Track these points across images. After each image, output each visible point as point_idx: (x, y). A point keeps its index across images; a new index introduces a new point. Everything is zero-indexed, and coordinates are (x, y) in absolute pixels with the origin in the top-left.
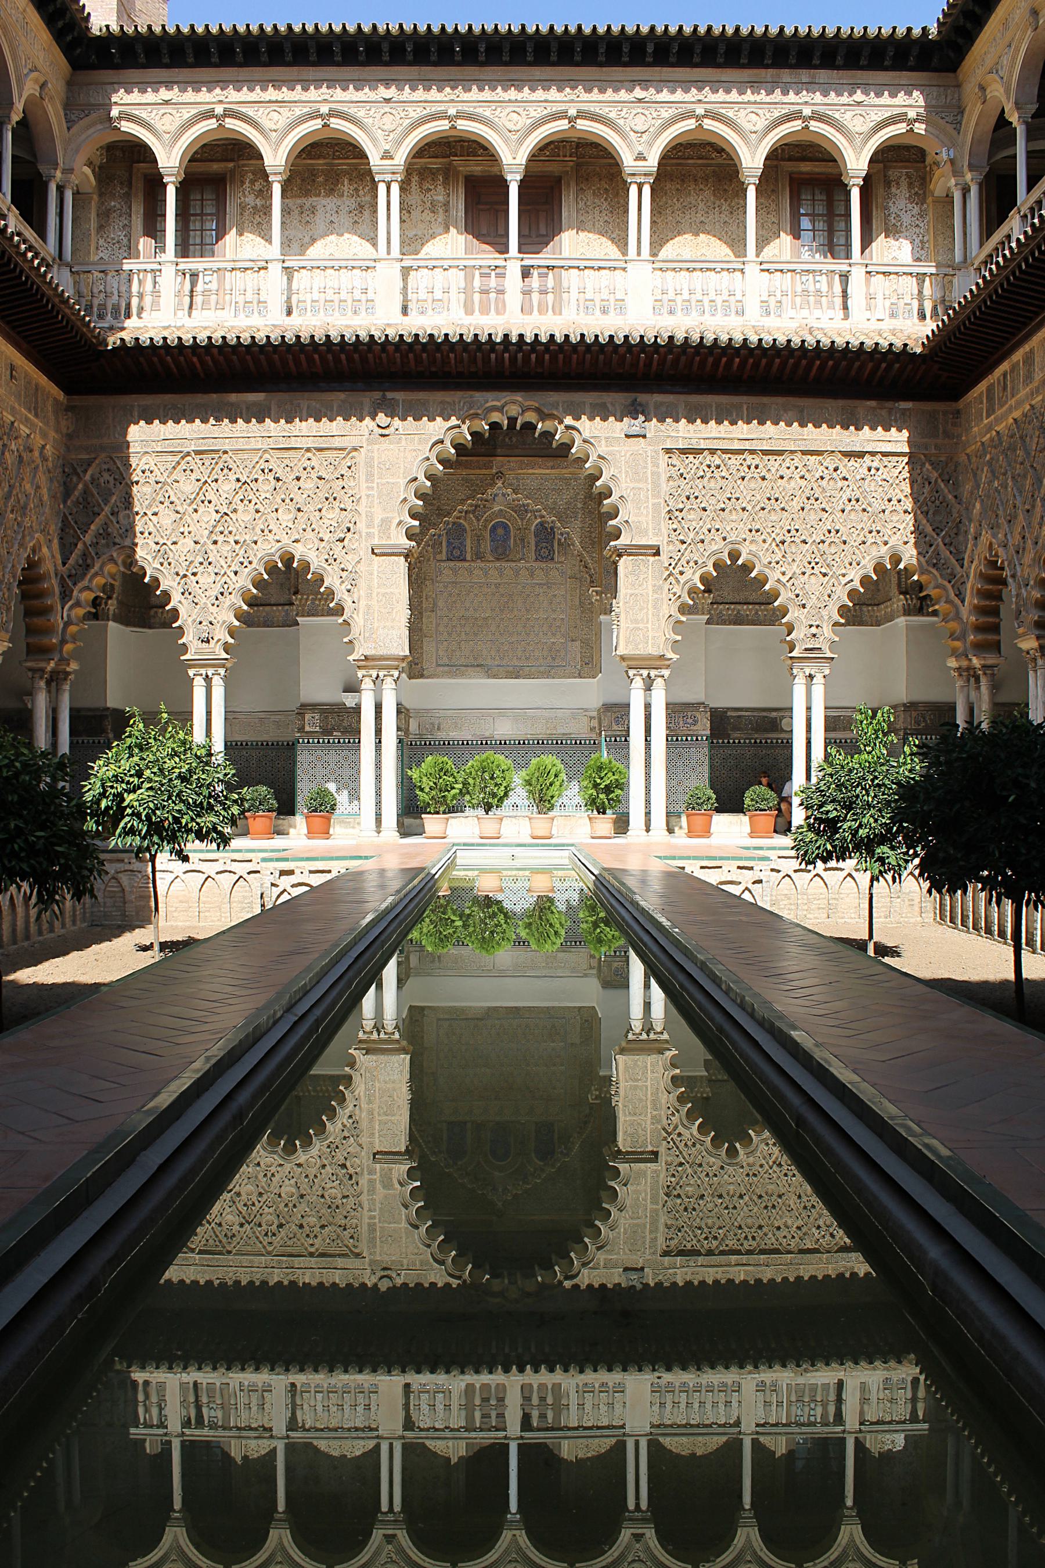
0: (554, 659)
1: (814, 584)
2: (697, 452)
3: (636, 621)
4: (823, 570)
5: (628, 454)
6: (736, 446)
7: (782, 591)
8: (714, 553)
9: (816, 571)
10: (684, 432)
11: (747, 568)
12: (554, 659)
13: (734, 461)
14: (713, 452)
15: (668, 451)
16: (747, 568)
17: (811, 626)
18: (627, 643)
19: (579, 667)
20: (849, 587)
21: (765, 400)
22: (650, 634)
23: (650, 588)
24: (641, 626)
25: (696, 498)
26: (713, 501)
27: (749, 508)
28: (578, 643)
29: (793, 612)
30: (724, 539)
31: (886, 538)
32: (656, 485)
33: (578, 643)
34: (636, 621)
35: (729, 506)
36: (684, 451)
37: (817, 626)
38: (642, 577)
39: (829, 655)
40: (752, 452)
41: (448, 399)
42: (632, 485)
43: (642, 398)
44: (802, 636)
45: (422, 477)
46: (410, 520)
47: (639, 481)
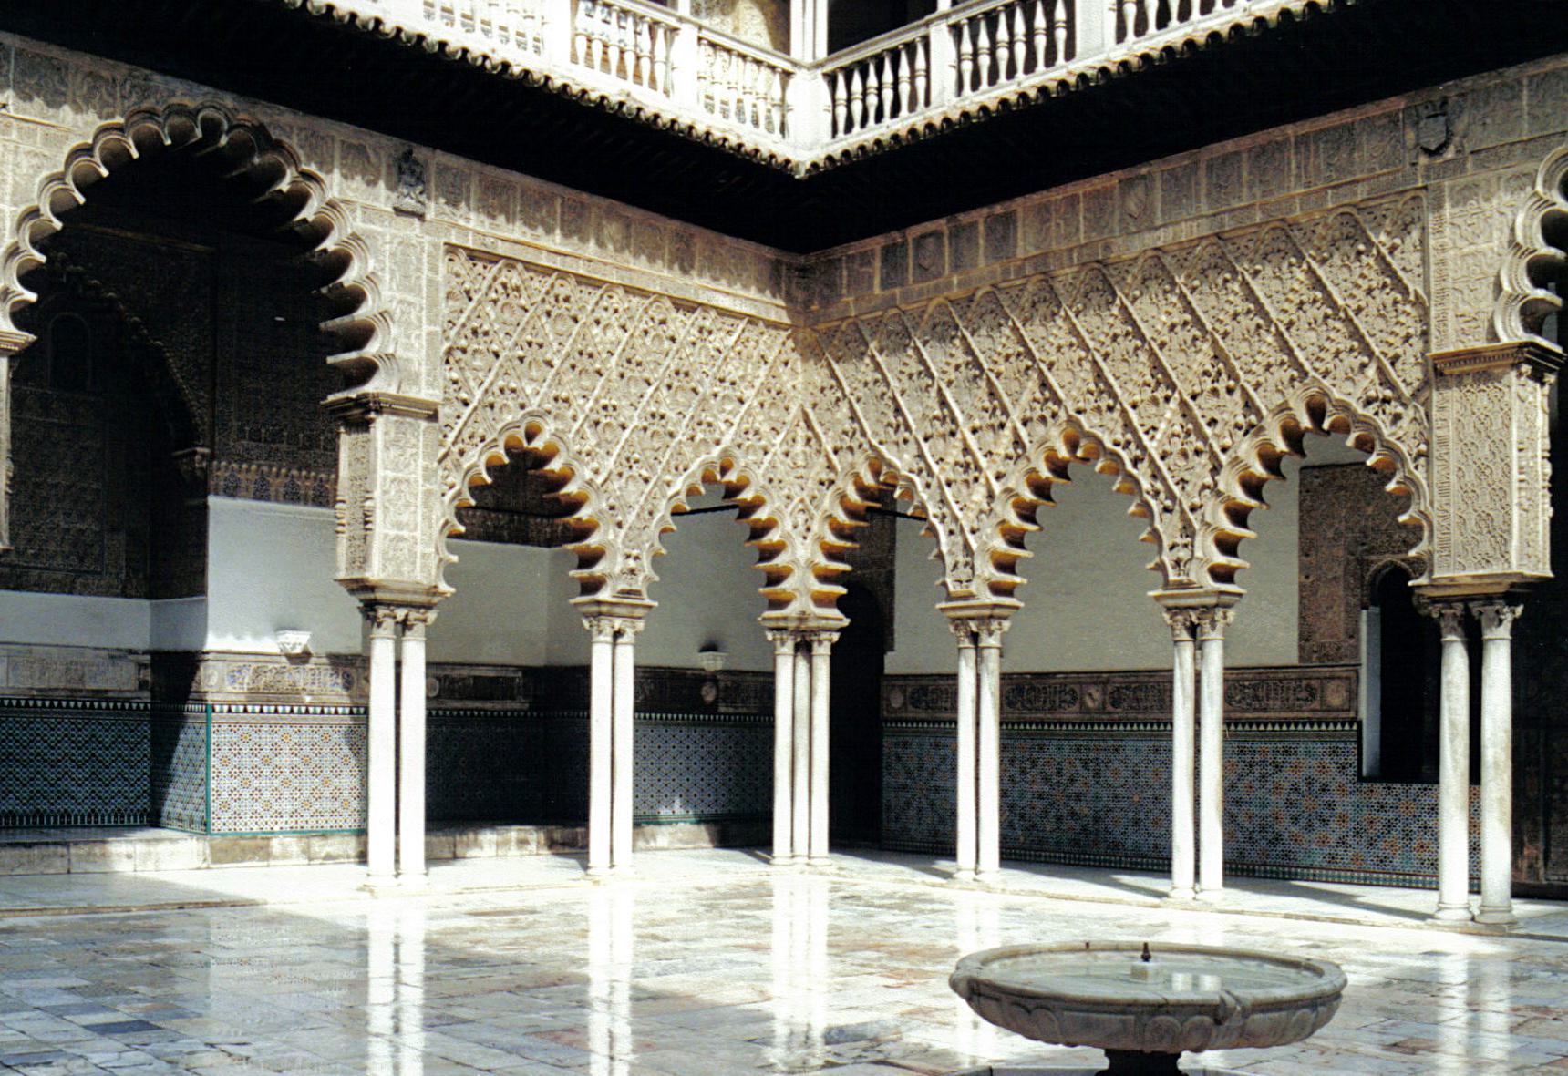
0: (81, 560)
1: (635, 494)
2: (493, 259)
3: (399, 526)
4: (645, 473)
5: (398, 244)
6: (544, 261)
7: (593, 496)
8: (507, 427)
9: (635, 471)
10: (474, 226)
11: (542, 459)
12: (81, 560)
13: (539, 285)
14: (511, 263)
15: (452, 249)
16: (542, 459)
17: (628, 557)
18: (386, 559)
19: (123, 576)
20: (674, 503)
21: (585, 196)
22: (419, 549)
23: (420, 471)
24: (405, 533)
25: (486, 333)
26: (509, 343)
27: (556, 362)
28: (122, 537)
29: (606, 532)
30: (522, 407)
31: (717, 436)
32: (433, 304)
33: (122, 537)
34: (399, 526)
35: (529, 354)
36: (473, 255)
37: (637, 558)
38: (410, 451)
39: (647, 602)
40: (563, 274)
41: (105, 74)
42: (398, 296)
43: (421, 153)
44: (617, 570)
45: (46, 211)
46: (19, 288)
47: (411, 291)
